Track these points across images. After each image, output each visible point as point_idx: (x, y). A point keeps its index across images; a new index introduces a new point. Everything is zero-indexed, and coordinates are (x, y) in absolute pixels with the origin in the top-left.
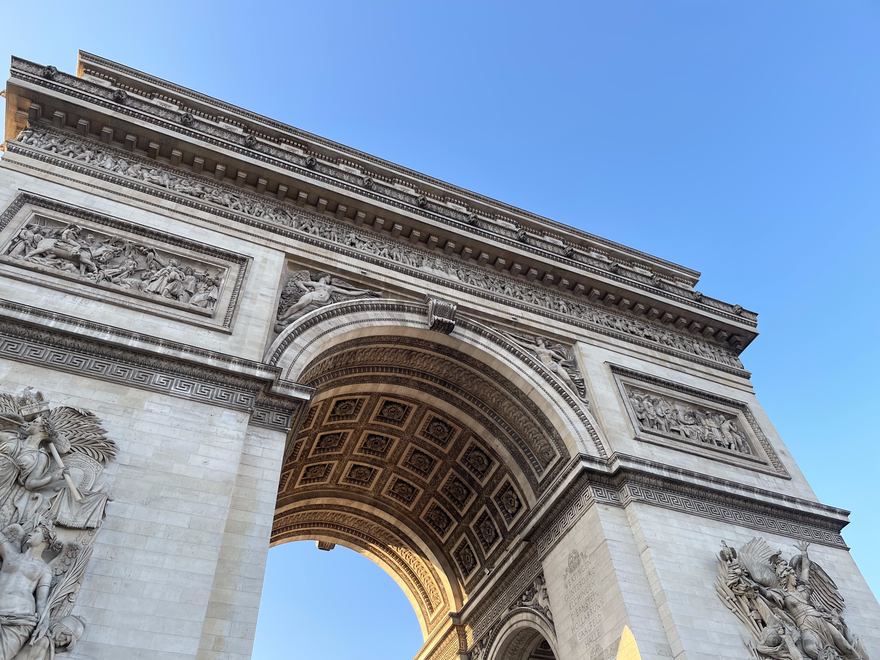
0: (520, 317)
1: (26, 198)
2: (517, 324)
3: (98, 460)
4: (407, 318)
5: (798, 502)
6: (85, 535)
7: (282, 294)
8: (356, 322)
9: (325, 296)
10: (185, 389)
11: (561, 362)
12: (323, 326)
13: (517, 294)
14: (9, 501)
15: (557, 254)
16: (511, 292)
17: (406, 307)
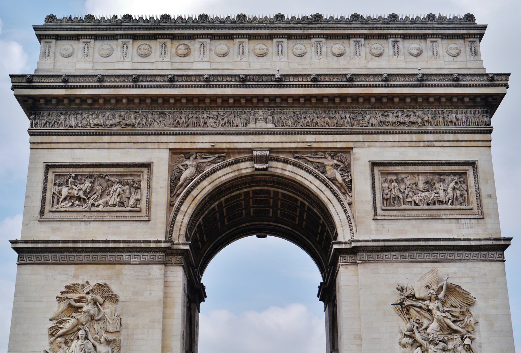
0: (312, 142)
1: (49, 167)
2: (311, 148)
3: (113, 302)
4: (241, 168)
5: (472, 240)
6: (117, 334)
7: (171, 179)
8: (212, 182)
9: (194, 171)
10: (136, 259)
11: (340, 168)
12: (194, 193)
13: (314, 121)
14: (91, 326)
15: (341, 81)
16: (310, 122)
17: (240, 160)
